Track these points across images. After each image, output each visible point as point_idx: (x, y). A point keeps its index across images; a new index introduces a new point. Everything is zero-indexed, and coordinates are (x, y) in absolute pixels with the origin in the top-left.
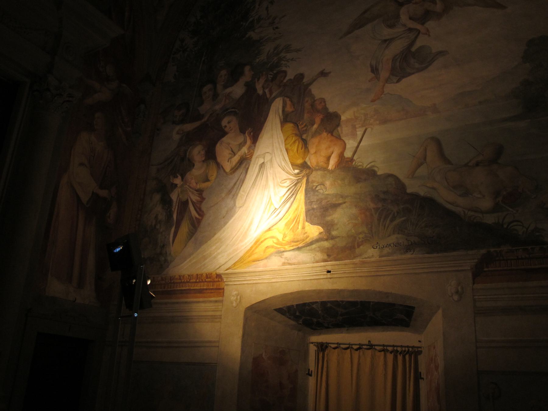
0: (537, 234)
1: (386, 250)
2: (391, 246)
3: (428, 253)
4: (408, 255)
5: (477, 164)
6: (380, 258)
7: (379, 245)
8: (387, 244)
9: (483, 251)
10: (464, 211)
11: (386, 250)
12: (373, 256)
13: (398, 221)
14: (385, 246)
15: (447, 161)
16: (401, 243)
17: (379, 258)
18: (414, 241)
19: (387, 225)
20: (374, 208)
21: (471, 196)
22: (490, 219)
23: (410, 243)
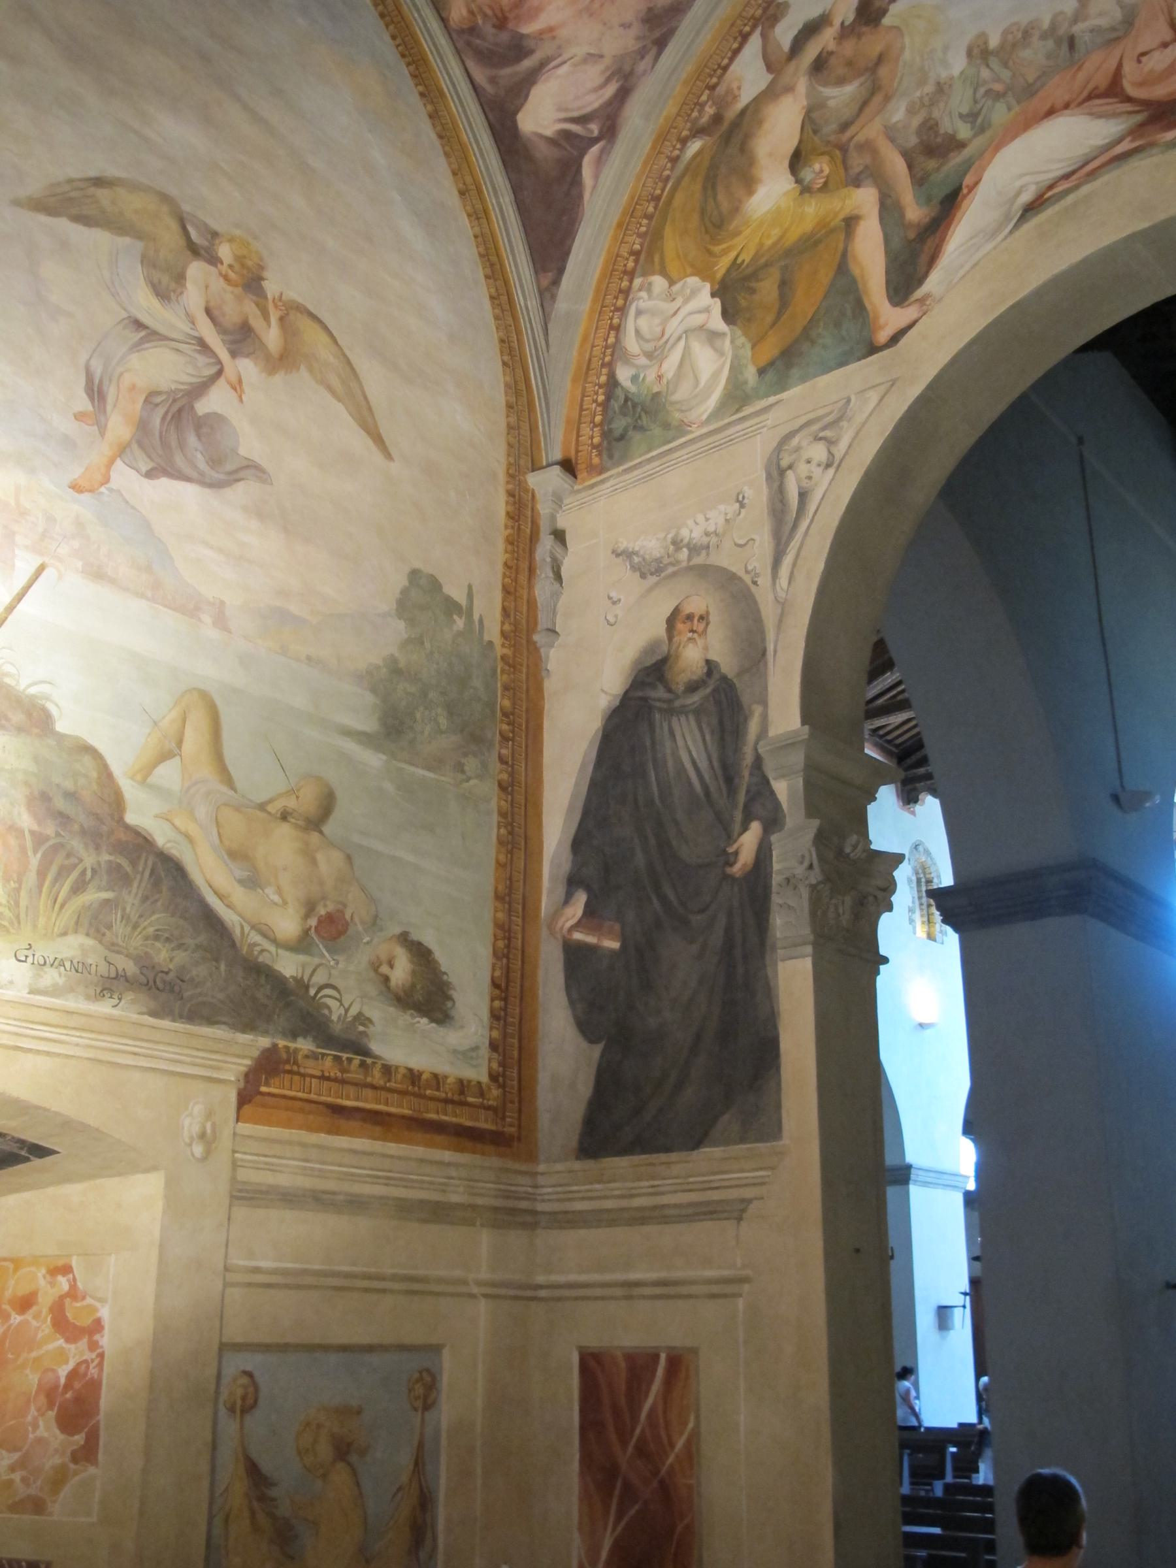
0: (361, 1028)
1: (52, 976)
2: (64, 966)
3: (154, 1014)
4: (105, 1008)
5: (284, 816)
6: (32, 996)
7: (34, 955)
8: (56, 958)
9: (265, 1042)
10: (242, 927)
11: (52, 976)
12: (11, 982)
13: (93, 896)
14: (48, 962)
15: (227, 779)
16: (91, 965)
17: (29, 993)
18: (124, 969)
19: (60, 900)
20: (32, 833)
21: (261, 892)
22: (288, 966)
23: (113, 975)
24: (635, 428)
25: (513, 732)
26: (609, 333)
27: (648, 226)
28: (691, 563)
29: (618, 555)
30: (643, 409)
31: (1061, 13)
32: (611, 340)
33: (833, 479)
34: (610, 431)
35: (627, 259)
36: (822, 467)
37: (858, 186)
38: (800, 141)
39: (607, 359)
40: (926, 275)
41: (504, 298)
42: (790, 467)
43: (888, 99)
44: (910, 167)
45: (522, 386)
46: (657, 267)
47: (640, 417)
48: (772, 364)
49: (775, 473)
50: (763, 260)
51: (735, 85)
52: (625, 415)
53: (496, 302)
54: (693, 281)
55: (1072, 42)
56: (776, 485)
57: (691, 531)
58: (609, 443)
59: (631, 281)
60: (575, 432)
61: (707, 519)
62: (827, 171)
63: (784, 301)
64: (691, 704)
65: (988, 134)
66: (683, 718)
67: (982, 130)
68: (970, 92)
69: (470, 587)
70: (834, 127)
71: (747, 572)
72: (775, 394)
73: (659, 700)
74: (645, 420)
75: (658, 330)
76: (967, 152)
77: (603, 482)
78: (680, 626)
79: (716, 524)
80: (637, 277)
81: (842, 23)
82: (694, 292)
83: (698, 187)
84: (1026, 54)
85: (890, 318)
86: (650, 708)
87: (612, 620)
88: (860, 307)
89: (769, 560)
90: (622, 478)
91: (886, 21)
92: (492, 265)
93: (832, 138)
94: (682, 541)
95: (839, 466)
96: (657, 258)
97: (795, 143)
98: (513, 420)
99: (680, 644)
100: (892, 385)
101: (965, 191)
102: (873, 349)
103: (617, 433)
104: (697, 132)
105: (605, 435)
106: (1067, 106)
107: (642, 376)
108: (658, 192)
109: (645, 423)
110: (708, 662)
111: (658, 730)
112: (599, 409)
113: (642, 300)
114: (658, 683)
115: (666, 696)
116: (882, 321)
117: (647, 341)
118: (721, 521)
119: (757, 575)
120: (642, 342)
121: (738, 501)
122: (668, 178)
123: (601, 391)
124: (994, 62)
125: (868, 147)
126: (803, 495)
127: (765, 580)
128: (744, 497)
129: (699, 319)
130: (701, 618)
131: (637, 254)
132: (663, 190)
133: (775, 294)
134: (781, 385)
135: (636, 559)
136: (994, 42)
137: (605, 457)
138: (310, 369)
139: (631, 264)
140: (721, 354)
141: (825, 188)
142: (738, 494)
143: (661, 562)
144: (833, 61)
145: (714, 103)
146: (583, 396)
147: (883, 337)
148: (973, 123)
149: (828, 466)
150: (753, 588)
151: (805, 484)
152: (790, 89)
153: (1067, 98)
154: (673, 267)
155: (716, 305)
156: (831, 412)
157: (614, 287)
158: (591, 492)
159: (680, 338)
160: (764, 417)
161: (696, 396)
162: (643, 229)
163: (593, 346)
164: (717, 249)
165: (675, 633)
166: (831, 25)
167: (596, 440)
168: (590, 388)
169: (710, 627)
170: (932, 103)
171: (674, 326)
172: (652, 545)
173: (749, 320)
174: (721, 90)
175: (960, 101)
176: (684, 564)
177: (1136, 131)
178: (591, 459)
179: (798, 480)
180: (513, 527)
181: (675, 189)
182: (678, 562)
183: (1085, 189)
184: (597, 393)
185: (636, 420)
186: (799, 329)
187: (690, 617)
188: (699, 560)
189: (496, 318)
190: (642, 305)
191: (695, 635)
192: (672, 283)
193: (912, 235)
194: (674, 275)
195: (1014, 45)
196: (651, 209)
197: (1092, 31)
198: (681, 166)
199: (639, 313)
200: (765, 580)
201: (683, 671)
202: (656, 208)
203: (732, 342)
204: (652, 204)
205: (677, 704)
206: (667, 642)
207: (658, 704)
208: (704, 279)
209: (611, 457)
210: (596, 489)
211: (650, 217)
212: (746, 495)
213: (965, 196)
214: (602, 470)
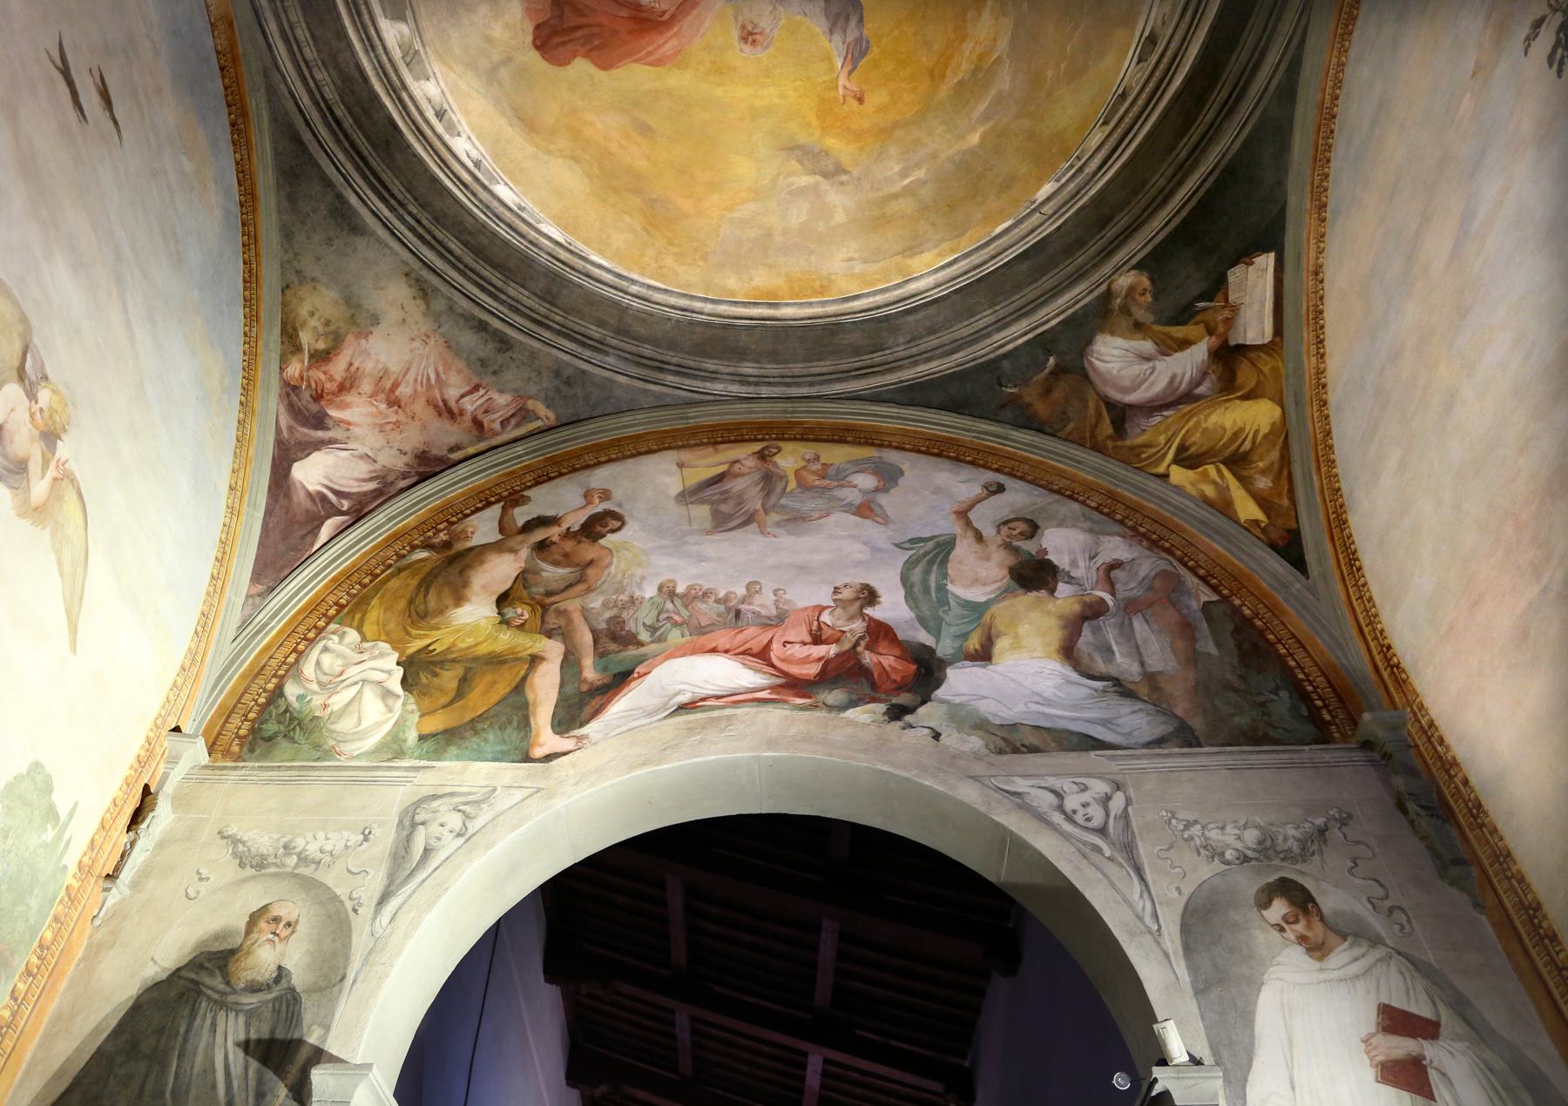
24: (285, 736)
25: (39, 968)
26: (291, 653)
27: (359, 591)
28: (296, 871)
29: (223, 837)
30: (299, 724)
31: (734, 593)
32: (291, 659)
33: (460, 848)
34: (260, 729)
35: (331, 607)
36: (454, 834)
37: (549, 638)
38: (511, 588)
39: (280, 672)
40: (587, 722)
41: (220, 583)
42: (423, 823)
43: (589, 590)
44: (595, 641)
45: (199, 657)
46: (355, 623)
47: (294, 729)
48: (433, 735)
49: (407, 823)
50: (453, 656)
51: (470, 530)
52: (279, 722)
53: (214, 582)
54: (385, 646)
55: (738, 614)
56: (405, 833)
57: (307, 843)
58: (254, 739)
59: (327, 624)
60: (225, 717)
61: (327, 839)
62: (526, 616)
63: (460, 694)
64: (246, 1004)
65: (663, 645)
66: (232, 1016)
67: (659, 640)
68: (654, 613)
69: (76, 804)
70: (542, 590)
71: (350, 898)
72: (428, 760)
73: (212, 989)
74: (297, 734)
75: (339, 669)
76: (642, 650)
77: (235, 768)
78: (262, 924)
79: (334, 846)
80: (334, 623)
81: (569, 528)
82: (382, 655)
83: (415, 582)
84: (701, 606)
85: (546, 739)
86: (199, 993)
87: (192, 893)
88: (525, 724)
89: (377, 896)
90: (255, 773)
91: (602, 541)
92: (224, 553)
93: (537, 597)
94: (294, 848)
95: (469, 839)
96: (358, 616)
97: (507, 586)
98: (180, 681)
99: (256, 941)
100: (537, 792)
101: (636, 675)
102: (527, 758)
103: (267, 734)
104: (427, 546)
105: (252, 731)
106: (726, 652)
107: (309, 698)
108: (378, 571)
109: (296, 737)
110: (280, 968)
111: (197, 1022)
112: (256, 708)
113: (333, 642)
114: (217, 972)
115: (222, 987)
116: (541, 740)
117: (325, 674)
118: (341, 845)
119: (360, 905)
120: (318, 672)
121: (363, 833)
122: (390, 566)
123: (264, 694)
124: (678, 602)
125: (562, 613)
126: (427, 851)
127: (366, 911)
128: (370, 833)
129: (380, 676)
130: (289, 924)
131: (342, 607)
132: (383, 572)
133: (454, 684)
134: (438, 754)
135: (241, 848)
136: (680, 589)
137: (245, 749)
138: (54, 535)
139: (332, 612)
140: (390, 710)
141: (521, 627)
142: (366, 828)
143: (266, 860)
144: (553, 548)
145: (448, 534)
146: (245, 692)
147: (538, 752)
148: (653, 634)
149: (459, 835)
150: (351, 914)
151: (433, 842)
152: (513, 551)
153: (727, 647)
154: (369, 628)
155: (400, 672)
156: (476, 793)
157: (311, 621)
158: (220, 772)
159: (356, 683)
160: (414, 774)
161: (354, 733)
162: (355, 592)
163: (271, 657)
164: (414, 632)
165: (255, 930)
166: (559, 526)
167: (242, 732)
168: (254, 688)
169: (294, 936)
170: (623, 608)
171: (353, 672)
172: (262, 841)
173: (424, 694)
174: (458, 528)
175: (646, 615)
176: (289, 870)
177: (773, 688)
178: (231, 745)
179: (427, 837)
180: (136, 771)
181: (392, 576)
182: (283, 865)
183: (727, 712)
184: (259, 695)
185: (289, 731)
186: (467, 718)
187: (276, 920)
188: (306, 871)
189: (208, 594)
190: (330, 644)
191: (276, 939)
192: (364, 639)
193: (584, 688)
194: (369, 635)
195: (695, 598)
196: (367, 580)
197: (754, 613)
198: (405, 562)
199: (326, 649)
200: (366, 911)
201: (251, 969)
202: (371, 582)
203: (404, 705)
204: (369, 577)
205: (231, 998)
206: (243, 934)
207: (209, 992)
208: (394, 648)
209: (252, 751)
210: (225, 772)
211: (364, 586)
212: (373, 831)
213: (635, 679)
214: (239, 758)
